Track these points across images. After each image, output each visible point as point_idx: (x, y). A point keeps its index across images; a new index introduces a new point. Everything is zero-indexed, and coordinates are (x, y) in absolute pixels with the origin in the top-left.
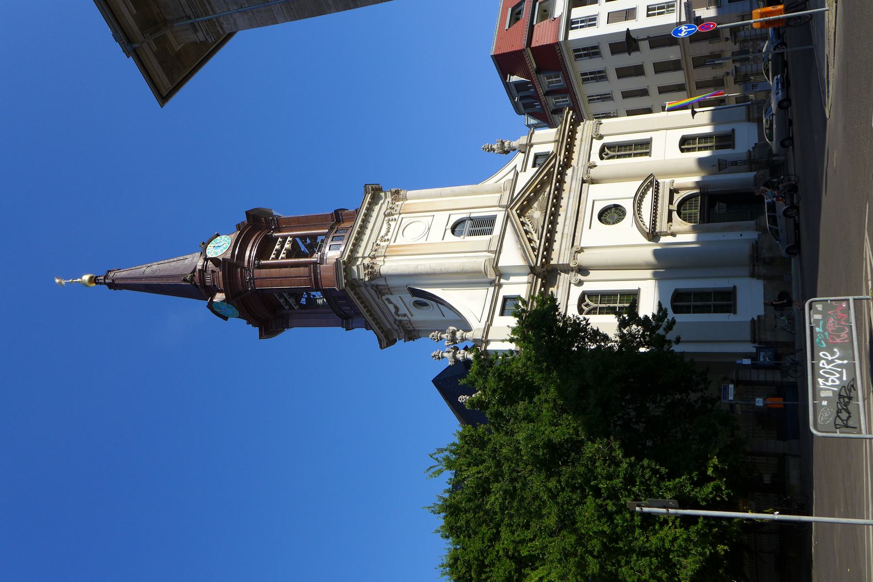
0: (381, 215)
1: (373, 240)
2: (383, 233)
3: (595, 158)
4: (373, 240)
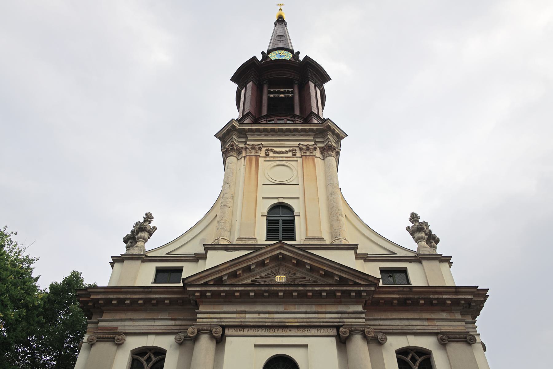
1: (265, 144)
2: (275, 149)
3: (396, 343)
4: (265, 144)
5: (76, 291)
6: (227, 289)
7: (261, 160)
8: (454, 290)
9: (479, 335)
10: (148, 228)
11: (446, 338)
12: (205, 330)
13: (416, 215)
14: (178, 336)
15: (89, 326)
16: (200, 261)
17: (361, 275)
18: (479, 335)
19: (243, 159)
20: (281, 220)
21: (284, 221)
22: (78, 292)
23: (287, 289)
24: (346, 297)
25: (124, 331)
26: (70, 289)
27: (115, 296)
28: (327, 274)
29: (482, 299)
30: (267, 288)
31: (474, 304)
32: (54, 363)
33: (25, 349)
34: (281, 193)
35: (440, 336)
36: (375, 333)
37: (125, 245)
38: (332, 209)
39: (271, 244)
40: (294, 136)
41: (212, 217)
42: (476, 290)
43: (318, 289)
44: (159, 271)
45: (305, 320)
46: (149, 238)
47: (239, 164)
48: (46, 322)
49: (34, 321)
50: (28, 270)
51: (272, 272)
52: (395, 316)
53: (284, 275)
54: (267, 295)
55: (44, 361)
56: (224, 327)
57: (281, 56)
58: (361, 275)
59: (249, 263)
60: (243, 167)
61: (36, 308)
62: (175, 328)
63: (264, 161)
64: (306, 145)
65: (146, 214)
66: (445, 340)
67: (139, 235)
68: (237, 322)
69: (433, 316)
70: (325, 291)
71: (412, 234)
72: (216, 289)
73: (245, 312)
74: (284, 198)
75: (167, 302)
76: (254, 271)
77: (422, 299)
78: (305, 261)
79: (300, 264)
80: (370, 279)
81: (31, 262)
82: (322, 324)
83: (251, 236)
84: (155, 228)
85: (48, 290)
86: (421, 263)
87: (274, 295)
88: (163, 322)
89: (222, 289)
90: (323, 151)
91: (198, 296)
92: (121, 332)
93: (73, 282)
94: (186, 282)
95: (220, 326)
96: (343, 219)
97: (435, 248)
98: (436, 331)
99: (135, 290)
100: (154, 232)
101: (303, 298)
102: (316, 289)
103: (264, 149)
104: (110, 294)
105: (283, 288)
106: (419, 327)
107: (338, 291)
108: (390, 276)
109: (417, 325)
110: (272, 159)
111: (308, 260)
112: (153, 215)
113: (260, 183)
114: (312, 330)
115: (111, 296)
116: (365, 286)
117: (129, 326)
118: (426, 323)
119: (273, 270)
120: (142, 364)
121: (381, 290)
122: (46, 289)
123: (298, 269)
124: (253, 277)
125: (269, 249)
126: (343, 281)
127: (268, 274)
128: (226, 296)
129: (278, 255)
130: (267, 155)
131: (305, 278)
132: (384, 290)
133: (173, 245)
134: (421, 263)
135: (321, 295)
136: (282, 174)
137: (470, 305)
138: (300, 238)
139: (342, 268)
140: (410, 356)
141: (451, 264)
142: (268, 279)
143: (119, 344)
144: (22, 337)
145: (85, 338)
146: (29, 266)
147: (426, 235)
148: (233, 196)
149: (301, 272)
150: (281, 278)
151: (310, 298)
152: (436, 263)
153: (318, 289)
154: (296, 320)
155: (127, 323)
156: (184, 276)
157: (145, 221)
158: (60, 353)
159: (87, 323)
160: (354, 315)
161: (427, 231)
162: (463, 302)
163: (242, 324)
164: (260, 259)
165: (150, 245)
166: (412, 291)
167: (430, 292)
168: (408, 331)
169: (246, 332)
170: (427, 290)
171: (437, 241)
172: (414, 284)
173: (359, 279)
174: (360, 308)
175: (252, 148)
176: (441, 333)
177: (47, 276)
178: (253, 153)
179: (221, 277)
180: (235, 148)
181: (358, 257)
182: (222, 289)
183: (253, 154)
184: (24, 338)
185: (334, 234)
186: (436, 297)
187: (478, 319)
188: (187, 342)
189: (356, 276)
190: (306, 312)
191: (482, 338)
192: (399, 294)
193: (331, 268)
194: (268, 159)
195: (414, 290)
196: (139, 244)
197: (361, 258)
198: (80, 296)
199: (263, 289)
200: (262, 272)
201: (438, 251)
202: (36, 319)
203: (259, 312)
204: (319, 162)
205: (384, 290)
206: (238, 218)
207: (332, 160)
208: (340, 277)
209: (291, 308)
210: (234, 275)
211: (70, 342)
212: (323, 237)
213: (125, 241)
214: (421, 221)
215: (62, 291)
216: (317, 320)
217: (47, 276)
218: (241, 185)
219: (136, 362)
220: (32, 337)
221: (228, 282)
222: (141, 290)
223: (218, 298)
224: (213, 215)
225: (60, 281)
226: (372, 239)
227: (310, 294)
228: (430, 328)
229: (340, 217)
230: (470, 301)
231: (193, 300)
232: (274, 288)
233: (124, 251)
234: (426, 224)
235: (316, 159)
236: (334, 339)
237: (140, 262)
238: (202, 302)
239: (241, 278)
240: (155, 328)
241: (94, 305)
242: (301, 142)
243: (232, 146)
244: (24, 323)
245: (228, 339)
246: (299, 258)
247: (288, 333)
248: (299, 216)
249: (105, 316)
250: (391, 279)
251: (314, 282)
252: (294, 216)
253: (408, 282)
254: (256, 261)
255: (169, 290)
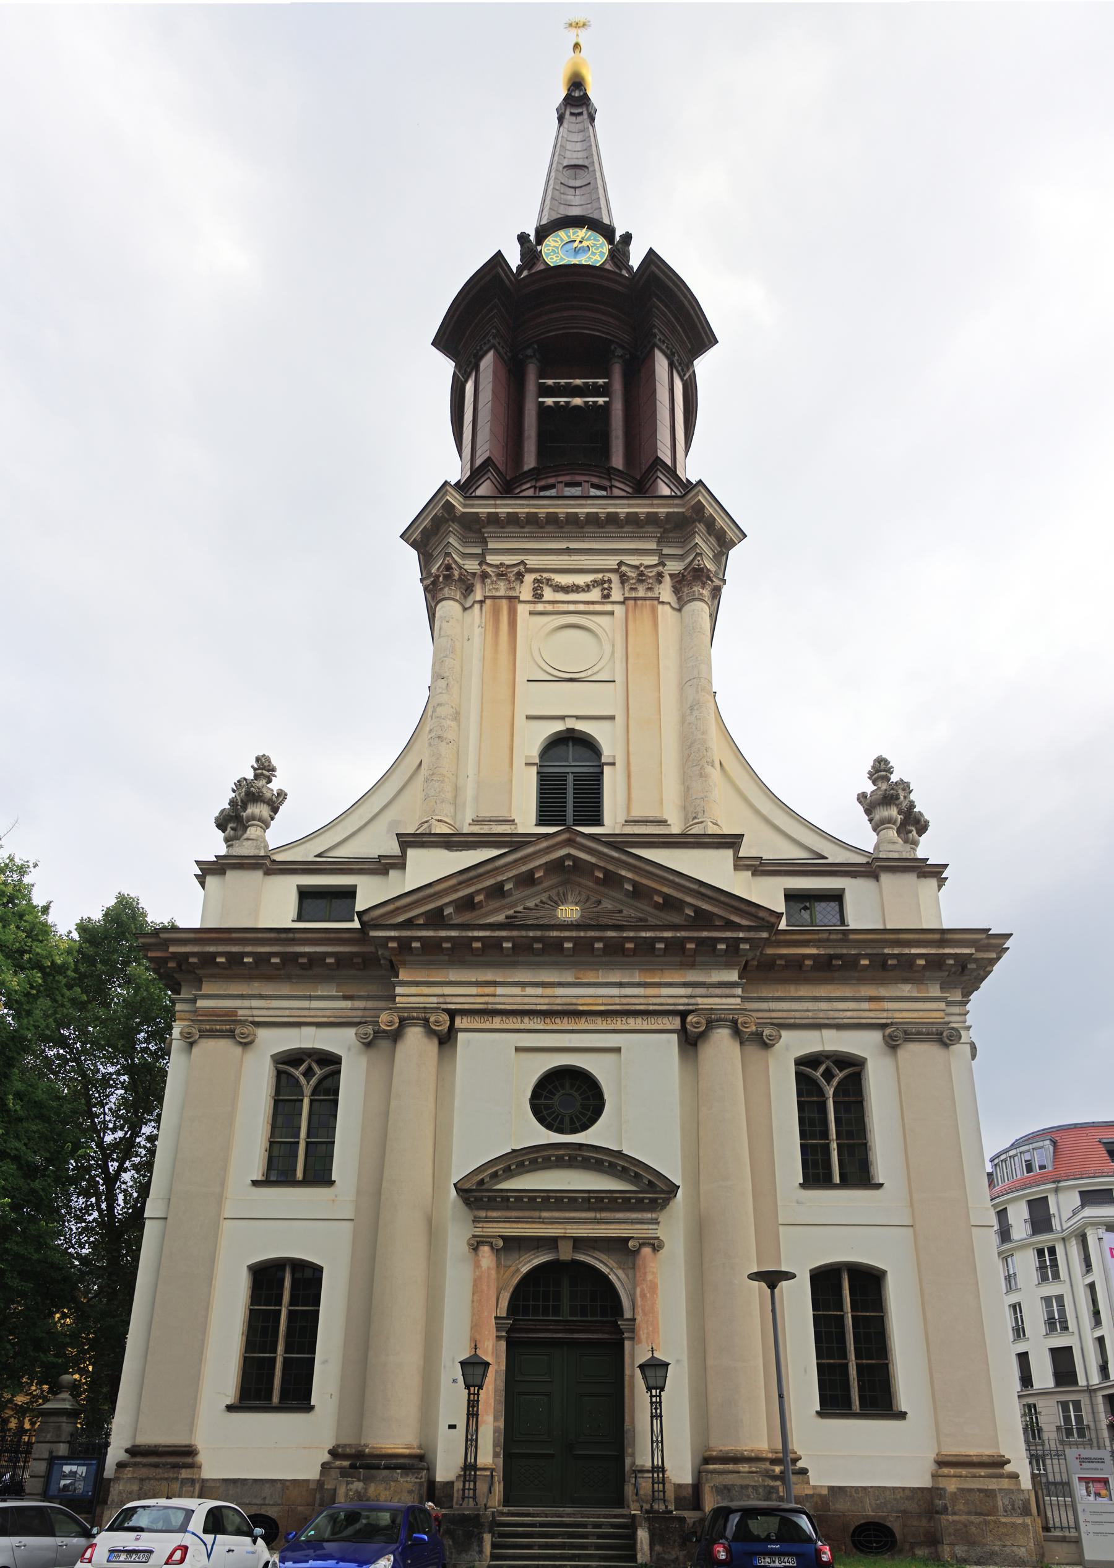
0: (612, 561)
1: (532, 561)
4: (532, 561)
5: (137, 936)
6: (453, 933)
7: (522, 610)
8: (937, 936)
9: (968, 1028)
10: (268, 795)
11: (901, 1034)
12: (414, 1018)
13: (886, 762)
14: (362, 1030)
15: (178, 1007)
16: (392, 872)
17: (743, 906)
18: (968, 1028)
19: (477, 606)
20: (571, 774)
21: (578, 778)
22: (141, 940)
23: (582, 934)
24: (704, 953)
25: (250, 1019)
26: (123, 933)
27: (220, 949)
28: (670, 904)
29: (994, 955)
30: (539, 933)
31: (974, 966)
32: (126, 1077)
33: (61, 1051)
34: (572, 705)
35: (888, 1031)
36: (758, 1024)
37: (220, 835)
38: (690, 747)
39: (548, 834)
40: (608, 537)
41: (412, 766)
42: (984, 936)
43: (649, 934)
44: (305, 894)
45: (617, 1000)
46: (272, 819)
47: (466, 621)
48: (89, 1001)
49: (63, 996)
50: (20, 892)
51: (550, 898)
52: (804, 991)
53: (576, 904)
54: (540, 947)
55: (104, 1075)
56: (452, 1014)
57: (577, 251)
58: (743, 906)
59: (500, 878)
60: (477, 631)
61: (61, 969)
62: (355, 1013)
63: (531, 613)
64: (637, 567)
65: (258, 759)
66: (896, 1037)
67: (249, 811)
68: (478, 1003)
69: (883, 992)
70: (661, 939)
71: (868, 812)
72: (430, 933)
73: (495, 984)
74: (578, 717)
75: (330, 960)
76: (511, 895)
77: (866, 956)
78: (623, 873)
79: (611, 880)
80: (761, 914)
81: (22, 870)
82: (651, 1008)
83: (502, 814)
84: (282, 795)
85: (75, 936)
86: (877, 878)
87: (556, 946)
88: (327, 1001)
89: (443, 933)
90: (680, 583)
91: (393, 948)
92: (246, 1021)
93: (124, 918)
94: (365, 918)
95: (444, 1010)
96: (715, 774)
97: (915, 843)
98: (884, 1021)
99: (260, 935)
100: (281, 803)
101: (616, 953)
102: (643, 934)
103: (529, 578)
104: (210, 945)
105: (574, 934)
106: (849, 1014)
107: (691, 940)
108: (805, 908)
109: (847, 1010)
110: (549, 608)
111: (630, 870)
112: (274, 762)
113: (521, 678)
114: (631, 1020)
115: (212, 949)
116: (749, 928)
117: (258, 1008)
118: (865, 1005)
119: (553, 893)
120: (297, 1080)
121: (782, 937)
122: (70, 932)
123: (606, 891)
124: (510, 908)
125: (544, 844)
126: (702, 919)
127: (542, 902)
128: (452, 949)
129: (562, 859)
130: (538, 596)
131: (620, 912)
132: (788, 937)
133: (327, 834)
134: (877, 878)
135: (654, 948)
136: (572, 650)
137: (964, 968)
138: (614, 818)
139: (703, 890)
140: (822, 1069)
141: (942, 882)
142: (542, 913)
143: (247, 1044)
144: (47, 1027)
145: (176, 1032)
146: (20, 881)
147: (899, 813)
148: (458, 713)
149: (613, 899)
150: (569, 912)
151: (628, 956)
152: (910, 879)
153: (649, 934)
154: (600, 1001)
155: (255, 1003)
156: (360, 906)
157: (256, 777)
158: (133, 1060)
159: (173, 1002)
160: (718, 988)
161: (904, 805)
162: (951, 962)
163: (490, 1007)
164: (524, 869)
165: (279, 834)
166: (846, 940)
167: (885, 941)
168: (827, 1021)
169: (497, 1022)
170: (879, 937)
171: (922, 827)
172: (854, 921)
173: (737, 915)
174: (733, 976)
175: (501, 575)
176: (892, 1024)
177: (69, 904)
178: (502, 589)
179: (440, 909)
180: (456, 573)
181: (740, 864)
182: (443, 933)
183: (501, 593)
184: (52, 1032)
185: (691, 808)
186: (896, 951)
187: (974, 996)
188: (381, 1039)
189: (732, 907)
190: (620, 985)
191: (973, 1035)
192: (818, 947)
193: (678, 890)
194: (540, 607)
195: (852, 937)
196: (252, 832)
197: (747, 868)
198: (146, 948)
199: (531, 934)
200: (529, 897)
201: (920, 853)
202: (68, 993)
203: (523, 985)
204: (665, 613)
205: (788, 937)
206: (471, 770)
207: (700, 610)
208: (697, 910)
209: (590, 977)
210: (467, 904)
211: (147, 1040)
212: (665, 817)
213: (221, 824)
214: (894, 778)
215: (106, 938)
216: (642, 1000)
217: (69, 904)
218: (475, 681)
219: (283, 1076)
220: (69, 1029)
221: (457, 920)
222: (273, 935)
223: (436, 953)
224: (411, 762)
225: (97, 916)
226: (777, 822)
227: (630, 945)
228: (871, 1014)
229: (709, 769)
230: (962, 961)
231: (385, 958)
232: (555, 934)
233: (222, 850)
234: (905, 786)
235: (660, 607)
236: (675, 1037)
237: (259, 874)
238: (404, 964)
239: (484, 910)
240: (312, 1013)
241: (179, 965)
242: (624, 558)
243: (448, 568)
244: (44, 1003)
245: (461, 1036)
246: (611, 867)
247: (582, 1024)
248: (613, 764)
249: (207, 989)
250: (806, 915)
251: (641, 920)
252: (601, 766)
253: (843, 921)
254: (514, 872)
255: (332, 935)
